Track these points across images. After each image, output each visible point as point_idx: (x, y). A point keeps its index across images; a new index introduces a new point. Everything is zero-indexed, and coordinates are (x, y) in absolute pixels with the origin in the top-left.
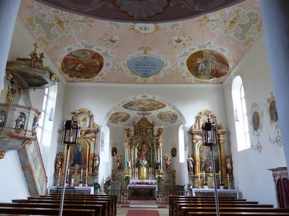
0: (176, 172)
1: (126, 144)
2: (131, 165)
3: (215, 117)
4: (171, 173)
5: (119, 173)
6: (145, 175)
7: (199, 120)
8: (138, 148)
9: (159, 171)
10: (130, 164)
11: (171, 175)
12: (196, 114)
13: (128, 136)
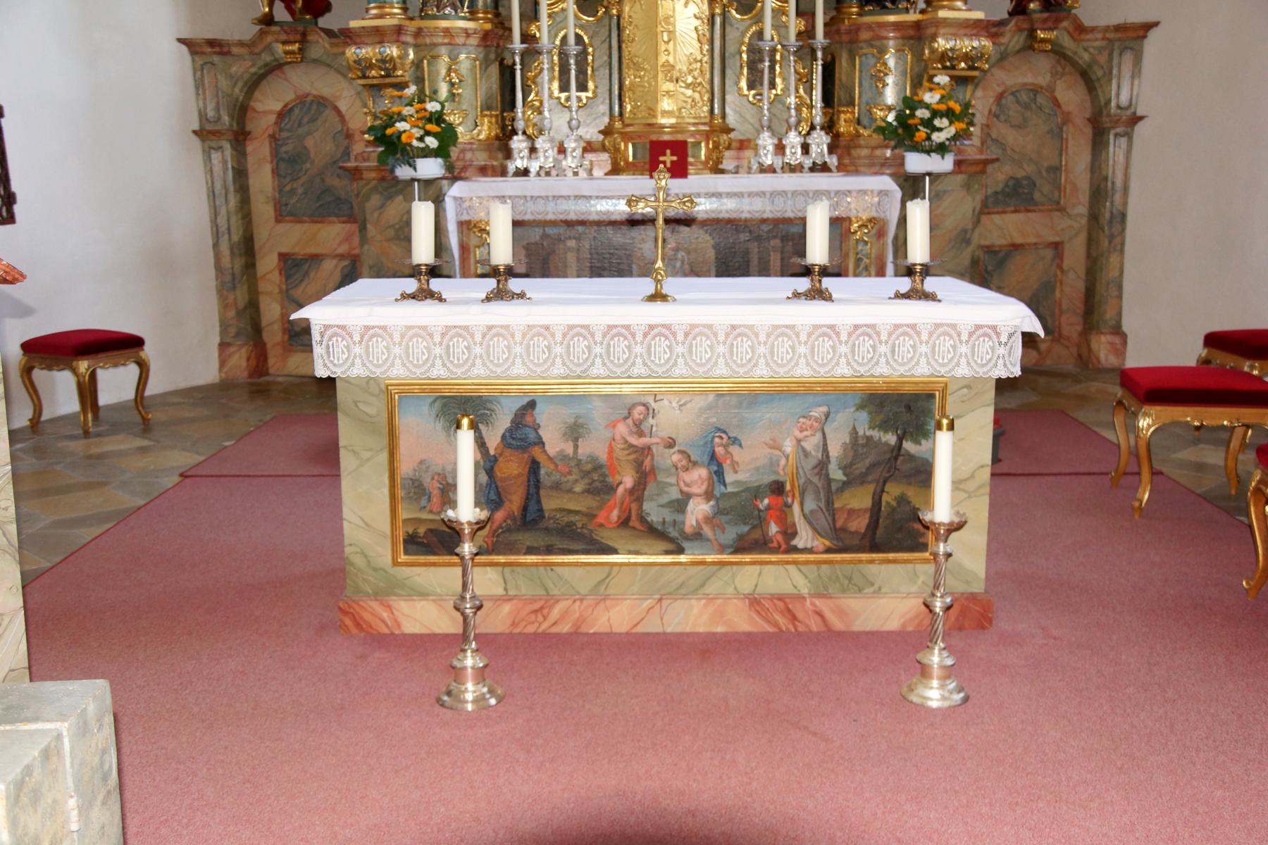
0: (1153, 45)
4: (1089, 80)
5: (303, 81)
9: (917, 35)
11: (1071, 96)
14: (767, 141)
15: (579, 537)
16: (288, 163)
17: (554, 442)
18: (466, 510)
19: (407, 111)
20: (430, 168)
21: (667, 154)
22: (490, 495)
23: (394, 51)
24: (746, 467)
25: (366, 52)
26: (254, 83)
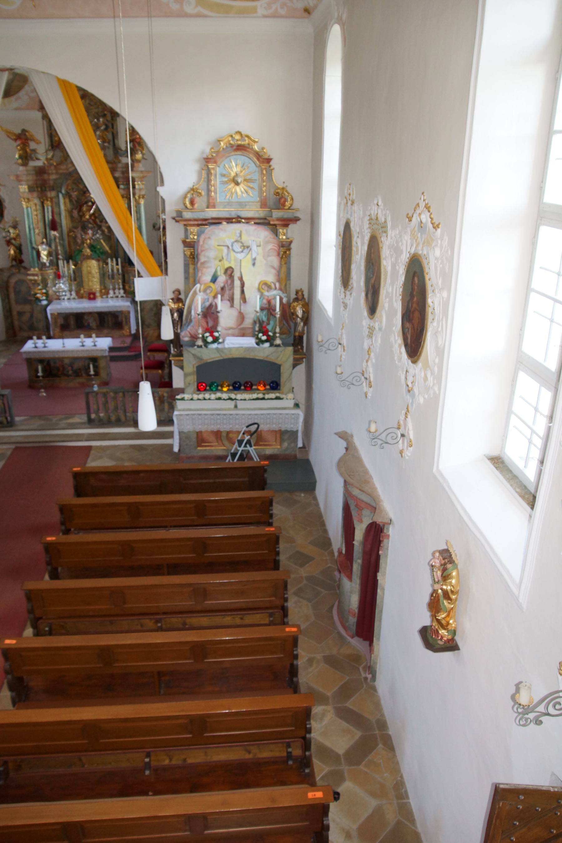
1: (24, 188)
2: (49, 254)
3: (269, 160)
6: (96, 287)
7: (209, 173)
8: (68, 195)
10: (44, 254)
12: (201, 147)
13: (26, 157)
14: (111, 292)
15: (56, 376)
16: (17, 293)
17: (52, 364)
18: (40, 374)
19: (39, 292)
20: (45, 303)
21: (92, 296)
22: (44, 371)
23: (36, 278)
24: (76, 366)
25: (32, 278)
26: (9, 277)
